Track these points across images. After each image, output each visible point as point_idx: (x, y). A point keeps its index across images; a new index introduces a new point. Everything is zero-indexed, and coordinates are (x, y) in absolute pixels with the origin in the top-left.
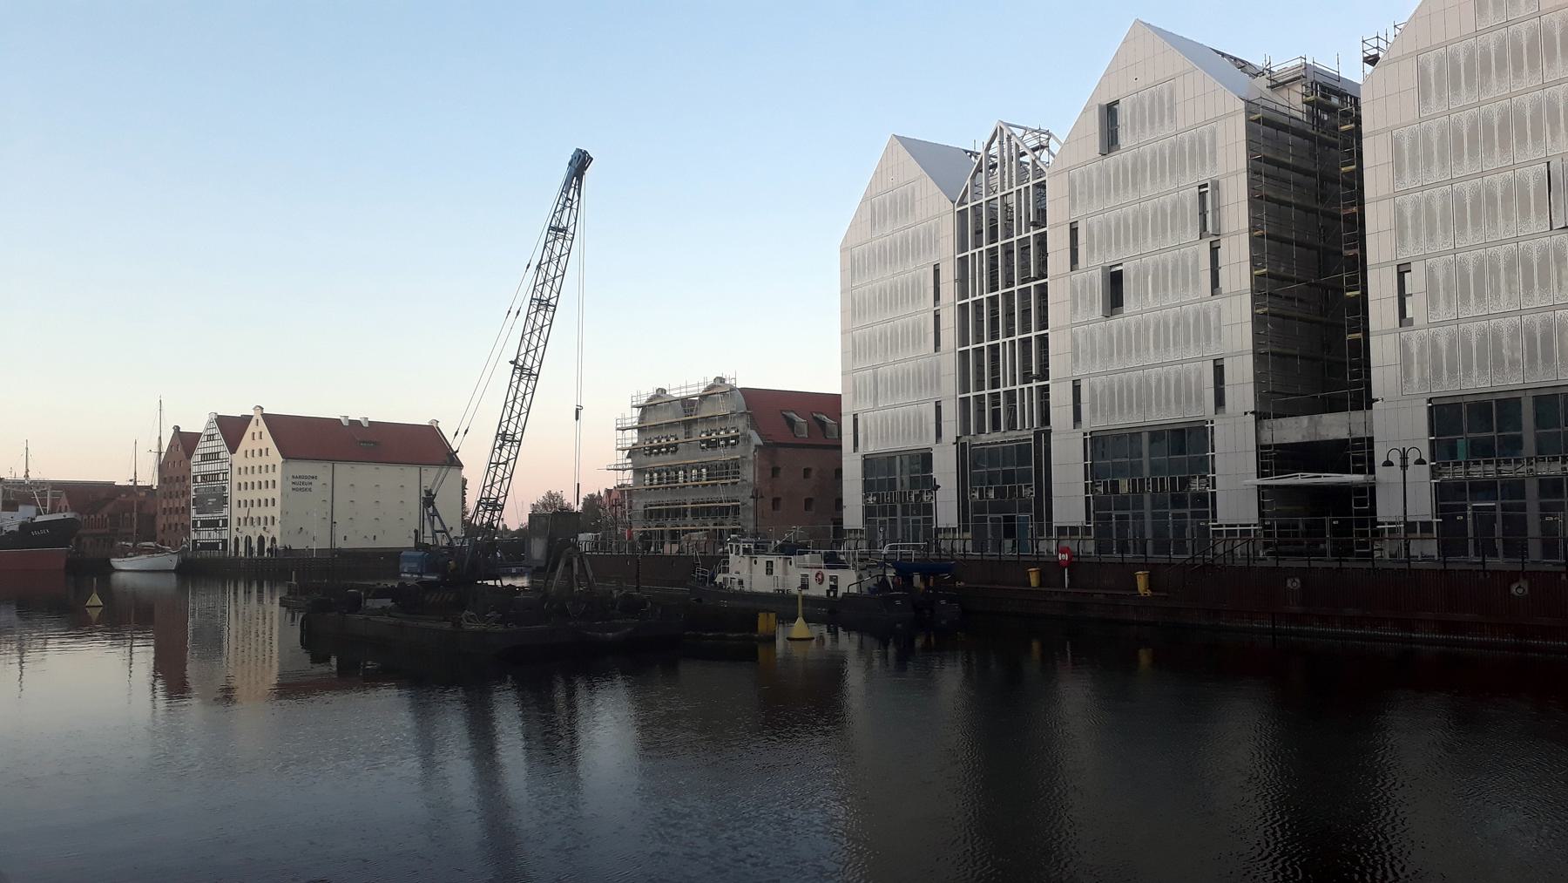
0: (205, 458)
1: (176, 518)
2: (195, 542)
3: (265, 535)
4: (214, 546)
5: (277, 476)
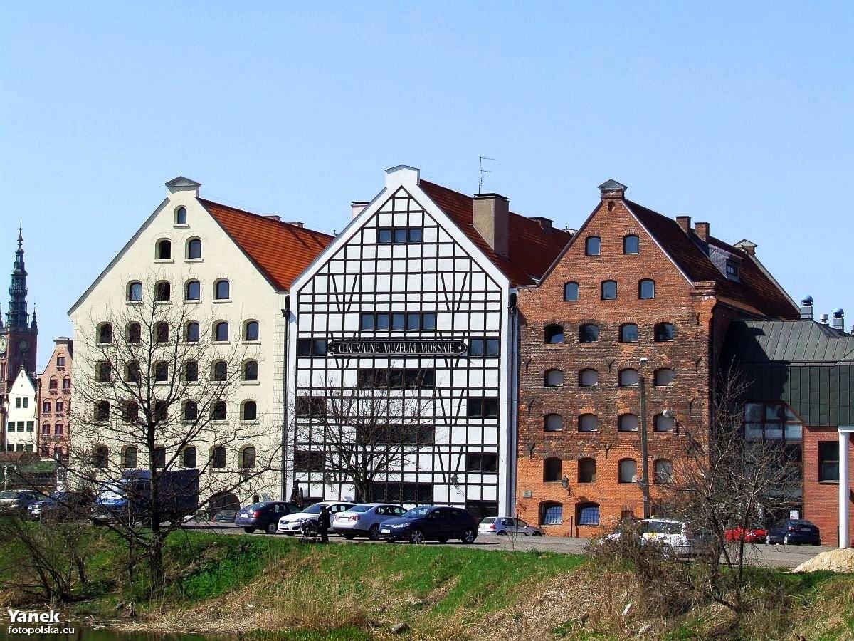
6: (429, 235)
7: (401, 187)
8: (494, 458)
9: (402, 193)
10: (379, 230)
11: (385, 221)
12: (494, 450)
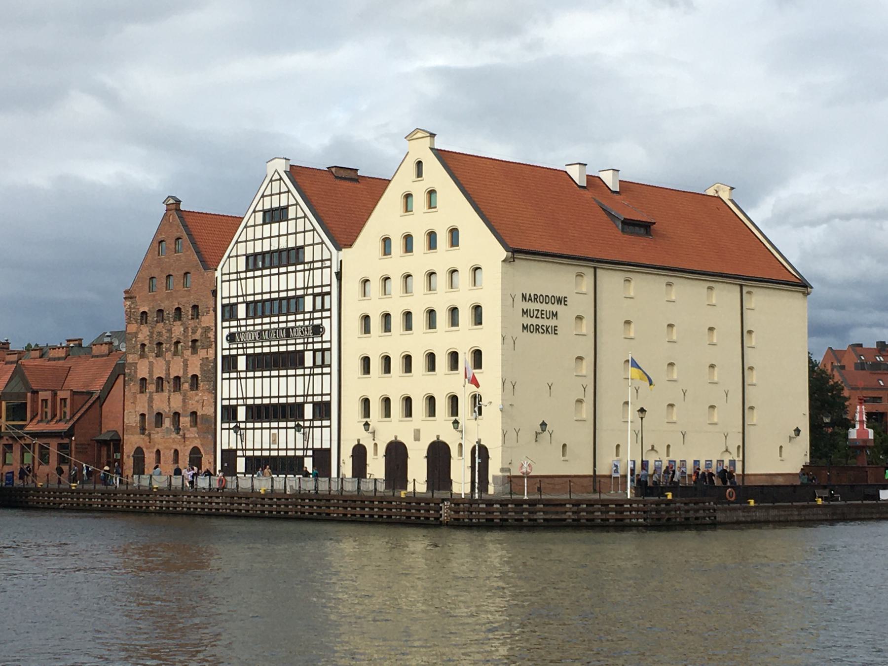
0: (258, 261)
1: (176, 402)
2: (230, 456)
3: (450, 438)
4: (289, 465)
5: (491, 293)
6: (291, 213)
7: (276, 171)
8: (328, 404)
9: (277, 177)
10: (265, 212)
11: (267, 206)
12: (326, 398)
